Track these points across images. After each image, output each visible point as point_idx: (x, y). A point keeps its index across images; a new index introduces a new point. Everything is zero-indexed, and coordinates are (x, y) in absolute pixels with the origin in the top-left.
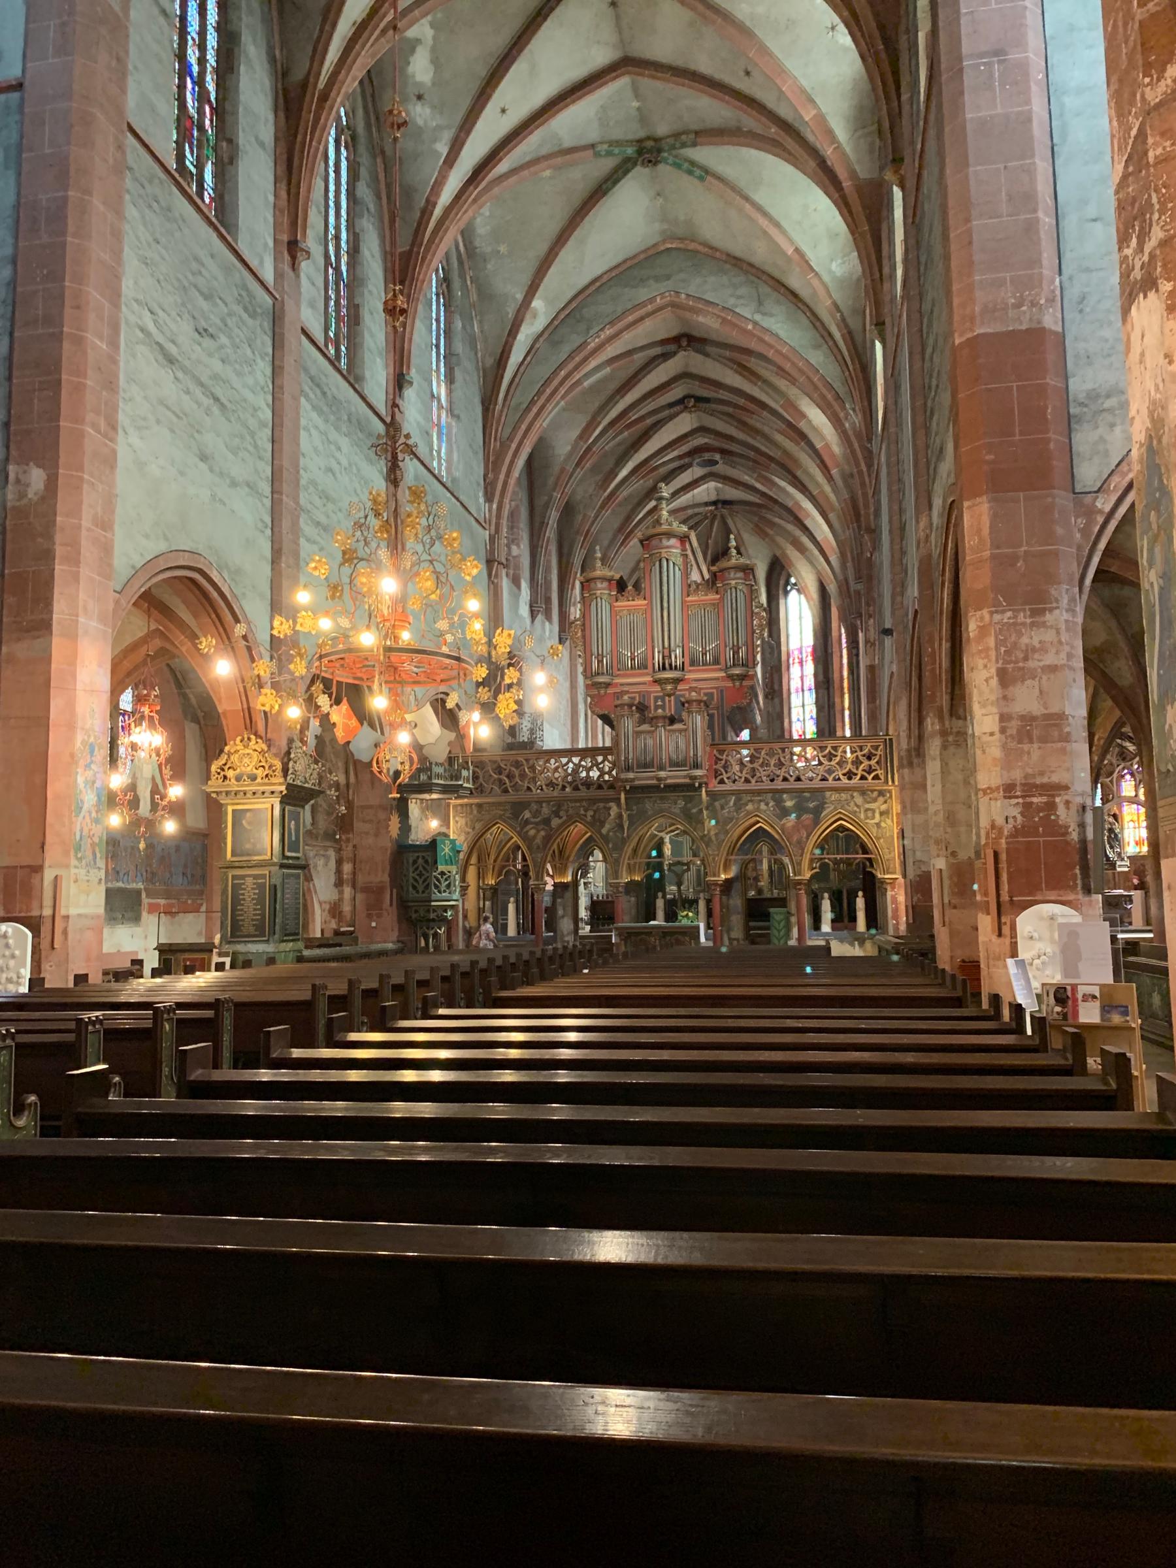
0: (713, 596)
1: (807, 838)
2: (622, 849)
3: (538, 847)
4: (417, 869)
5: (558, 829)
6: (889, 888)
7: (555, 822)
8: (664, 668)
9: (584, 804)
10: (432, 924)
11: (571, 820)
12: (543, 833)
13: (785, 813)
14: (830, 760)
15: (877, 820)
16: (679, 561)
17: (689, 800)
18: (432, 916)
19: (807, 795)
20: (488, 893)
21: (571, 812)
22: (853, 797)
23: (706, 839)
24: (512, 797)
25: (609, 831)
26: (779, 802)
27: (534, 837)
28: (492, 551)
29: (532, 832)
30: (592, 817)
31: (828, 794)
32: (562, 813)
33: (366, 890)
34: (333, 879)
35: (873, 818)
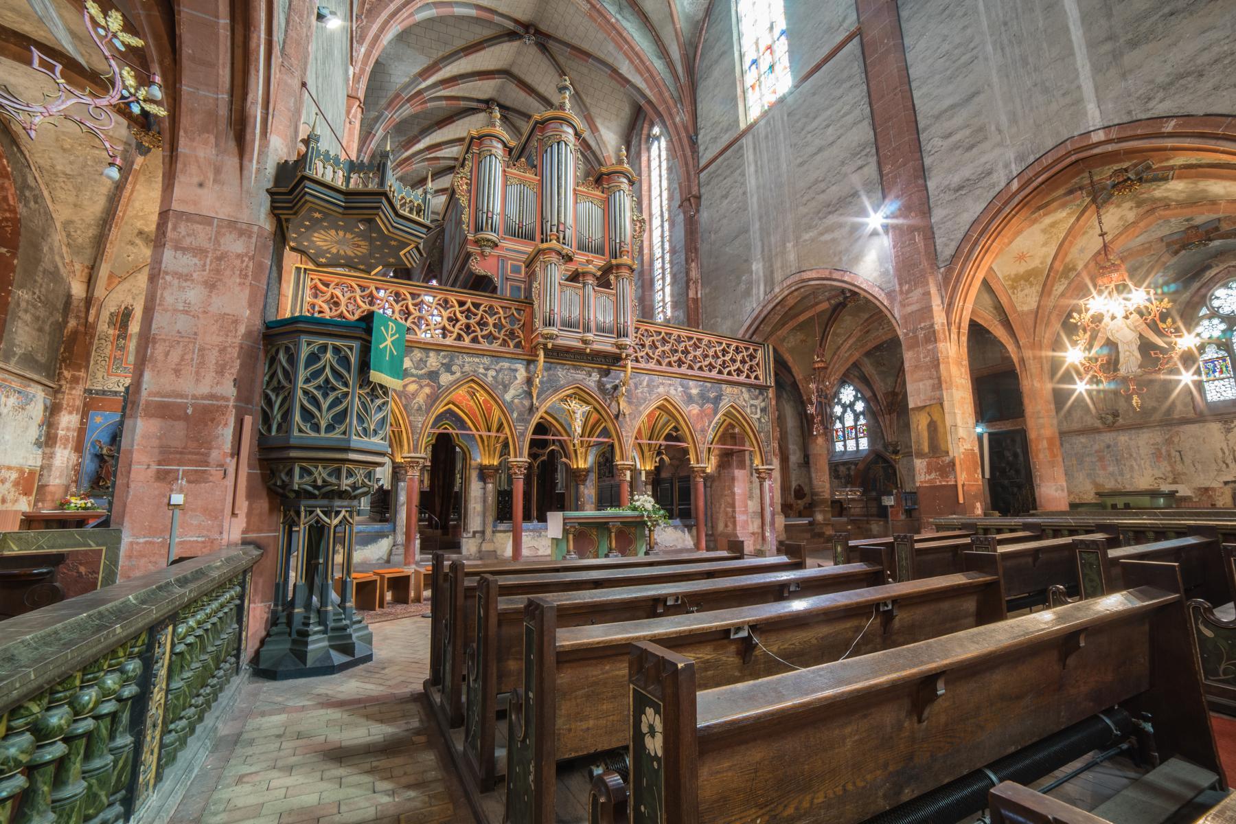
3: (420, 409)
4: (316, 374)
5: (448, 388)
7: (445, 379)
9: (486, 360)
10: (337, 503)
12: (427, 390)
13: (690, 399)
14: (724, 356)
15: (758, 416)
18: (346, 483)
19: (709, 385)
25: (513, 398)
26: (686, 388)
27: (415, 395)
29: (412, 388)
31: (724, 386)
32: (454, 368)
33: (165, 411)
34: (34, 432)
35: (756, 414)
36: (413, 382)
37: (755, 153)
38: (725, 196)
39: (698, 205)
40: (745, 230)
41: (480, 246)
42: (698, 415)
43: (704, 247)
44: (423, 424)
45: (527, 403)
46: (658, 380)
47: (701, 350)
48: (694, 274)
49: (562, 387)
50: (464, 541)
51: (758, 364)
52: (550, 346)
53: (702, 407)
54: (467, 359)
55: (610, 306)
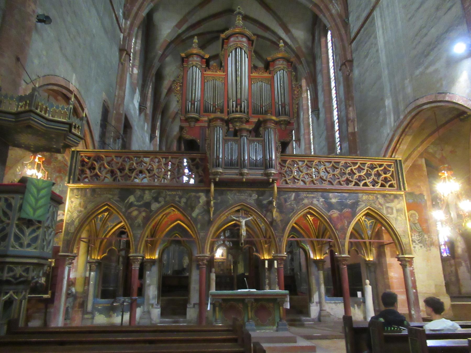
0: (266, 75)
1: (348, 227)
2: (208, 230)
3: (139, 226)
6: (408, 264)
7: (155, 206)
8: (237, 111)
9: (180, 193)
11: (168, 204)
12: (144, 214)
14: (359, 172)
16: (247, 51)
17: (261, 194)
19: (346, 195)
20: (94, 266)
21: (168, 198)
22: (377, 198)
23: (274, 224)
24: (122, 182)
25: (198, 215)
26: (327, 199)
27: (136, 217)
28: (124, 45)
29: (135, 213)
30: (186, 203)
31: (360, 195)
32: (160, 199)
35: (392, 213)
36: (136, 210)
37: (382, 20)
38: (366, 56)
39: (352, 66)
40: (379, 77)
41: (188, 122)
42: (337, 218)
43: (356, 95)
44: (141, 235)
45: (206, 218)
46: (303, 195)
47: (339, 170)
48: (352, 115)
49: (231, 205)
50: (188, 310)
51: (392, 176)
52: (217, 180)
53: (341, 210)
54: (168, 193)
55: (259, 147)
